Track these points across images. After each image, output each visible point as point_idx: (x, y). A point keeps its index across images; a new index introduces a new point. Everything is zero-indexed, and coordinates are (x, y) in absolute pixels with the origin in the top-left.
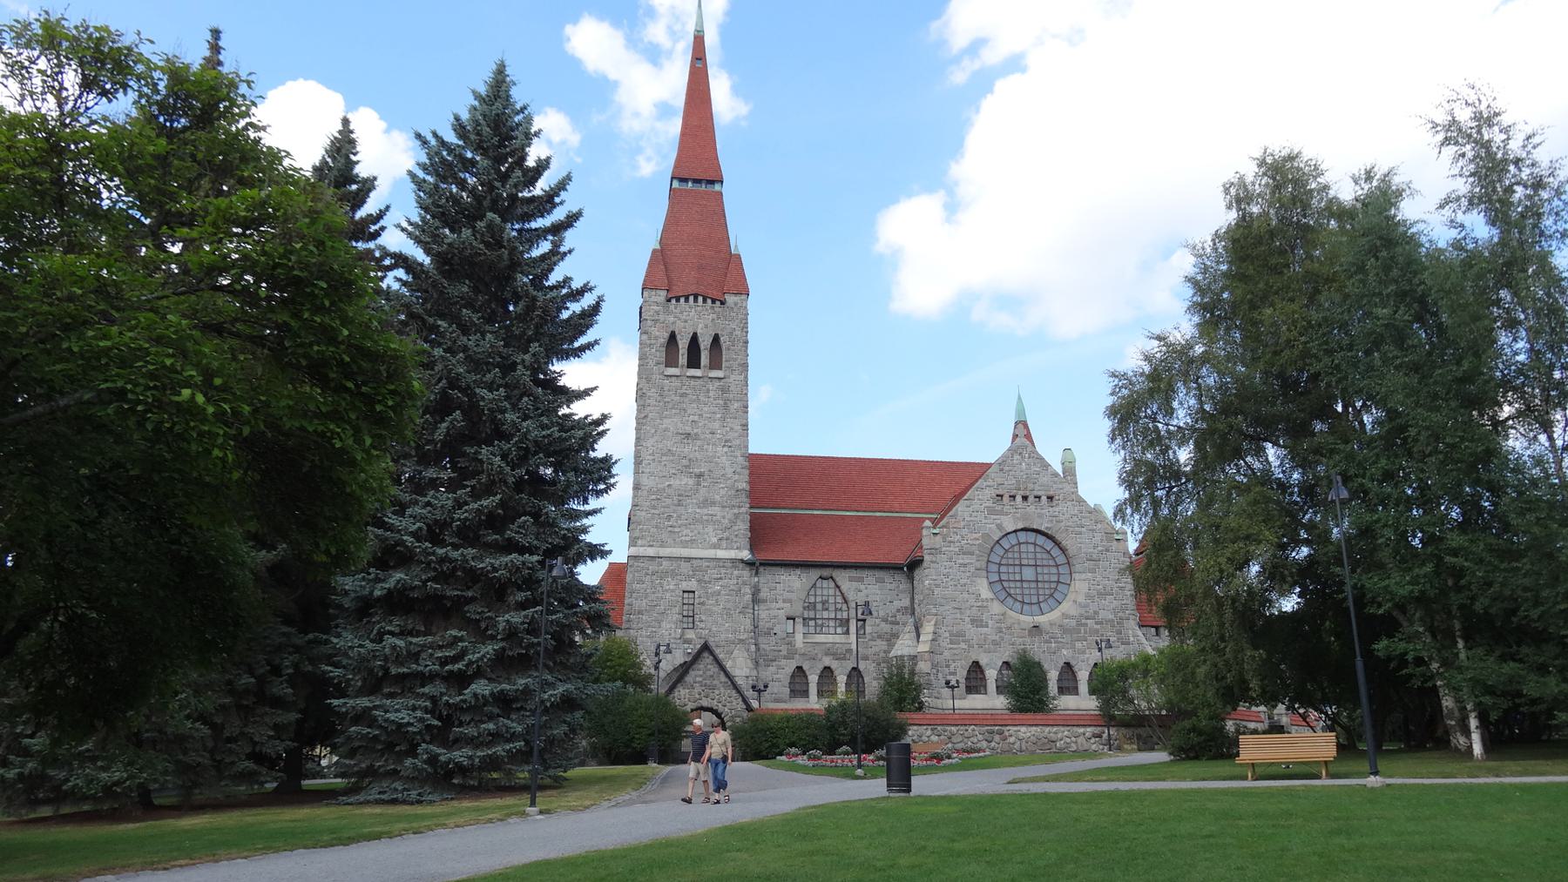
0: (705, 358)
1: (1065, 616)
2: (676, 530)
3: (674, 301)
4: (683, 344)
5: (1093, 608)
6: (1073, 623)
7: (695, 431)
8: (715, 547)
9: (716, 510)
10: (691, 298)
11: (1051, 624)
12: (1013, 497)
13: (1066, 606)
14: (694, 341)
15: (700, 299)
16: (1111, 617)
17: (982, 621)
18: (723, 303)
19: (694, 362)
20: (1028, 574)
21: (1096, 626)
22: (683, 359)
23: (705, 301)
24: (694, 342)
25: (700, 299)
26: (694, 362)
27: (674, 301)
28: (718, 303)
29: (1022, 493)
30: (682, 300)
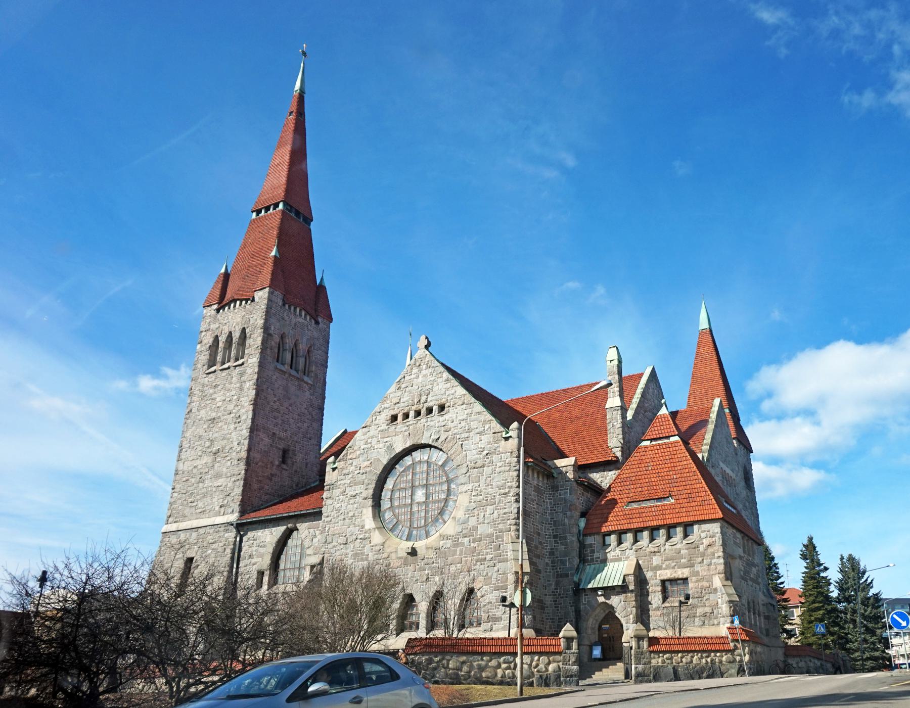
1: (443, 537)
2: (195, 504)
5: (472, 522)
6: (449, 543)
7: (219, 415)
8: (218, 514)
9: (221, 481)
11: (427, 548)
12: (406, 416)
13: (449, 528)
16: (490, 531)
17: (363, 554)
20: (420, 495)
21: (473, 545)
29: (414, 408)
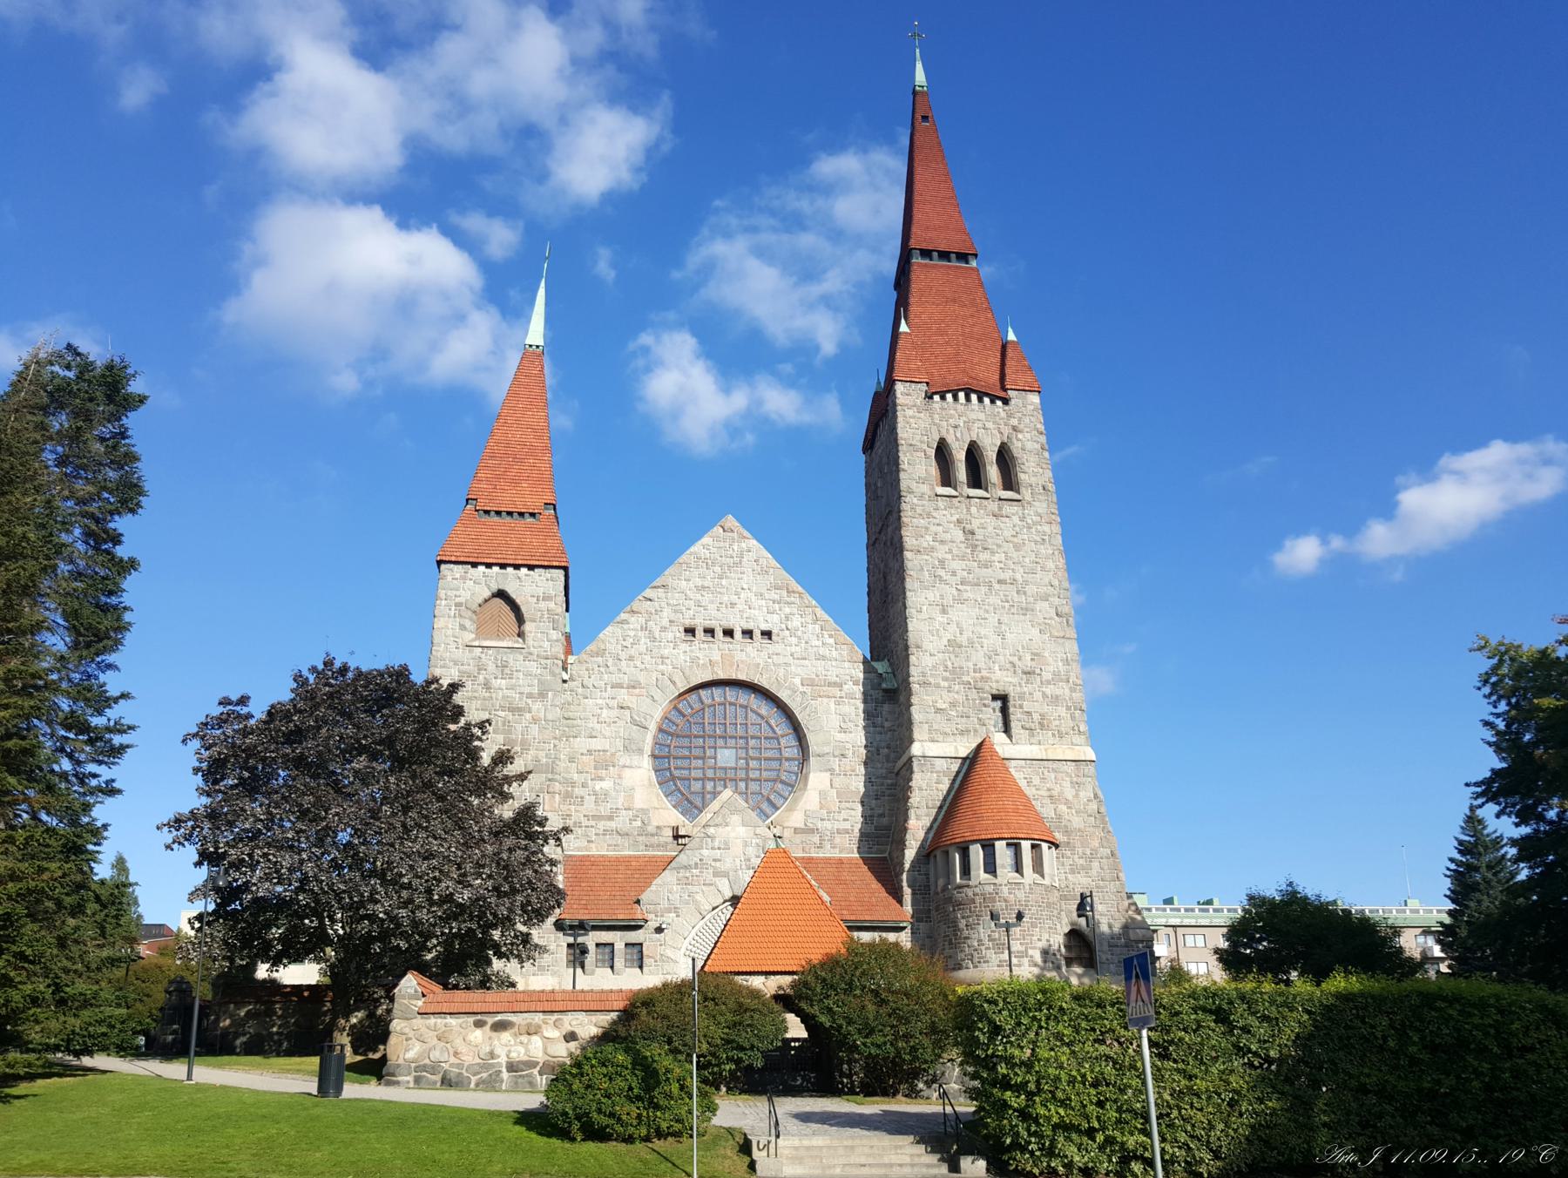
0: (993, 473)
3: (936, 398)
4: (960, 456)
10: (961, 395)
14: (973, 454)
15: (974, 397)
18: (1006, 401)
19: (976, 478)
22: (961, 473)
23: (980, 400)
24: (973, 454)
25: (974, 397)
26: (976, 478)
27: (936, 398)
28: (999, 403)
30: (949, 396)
